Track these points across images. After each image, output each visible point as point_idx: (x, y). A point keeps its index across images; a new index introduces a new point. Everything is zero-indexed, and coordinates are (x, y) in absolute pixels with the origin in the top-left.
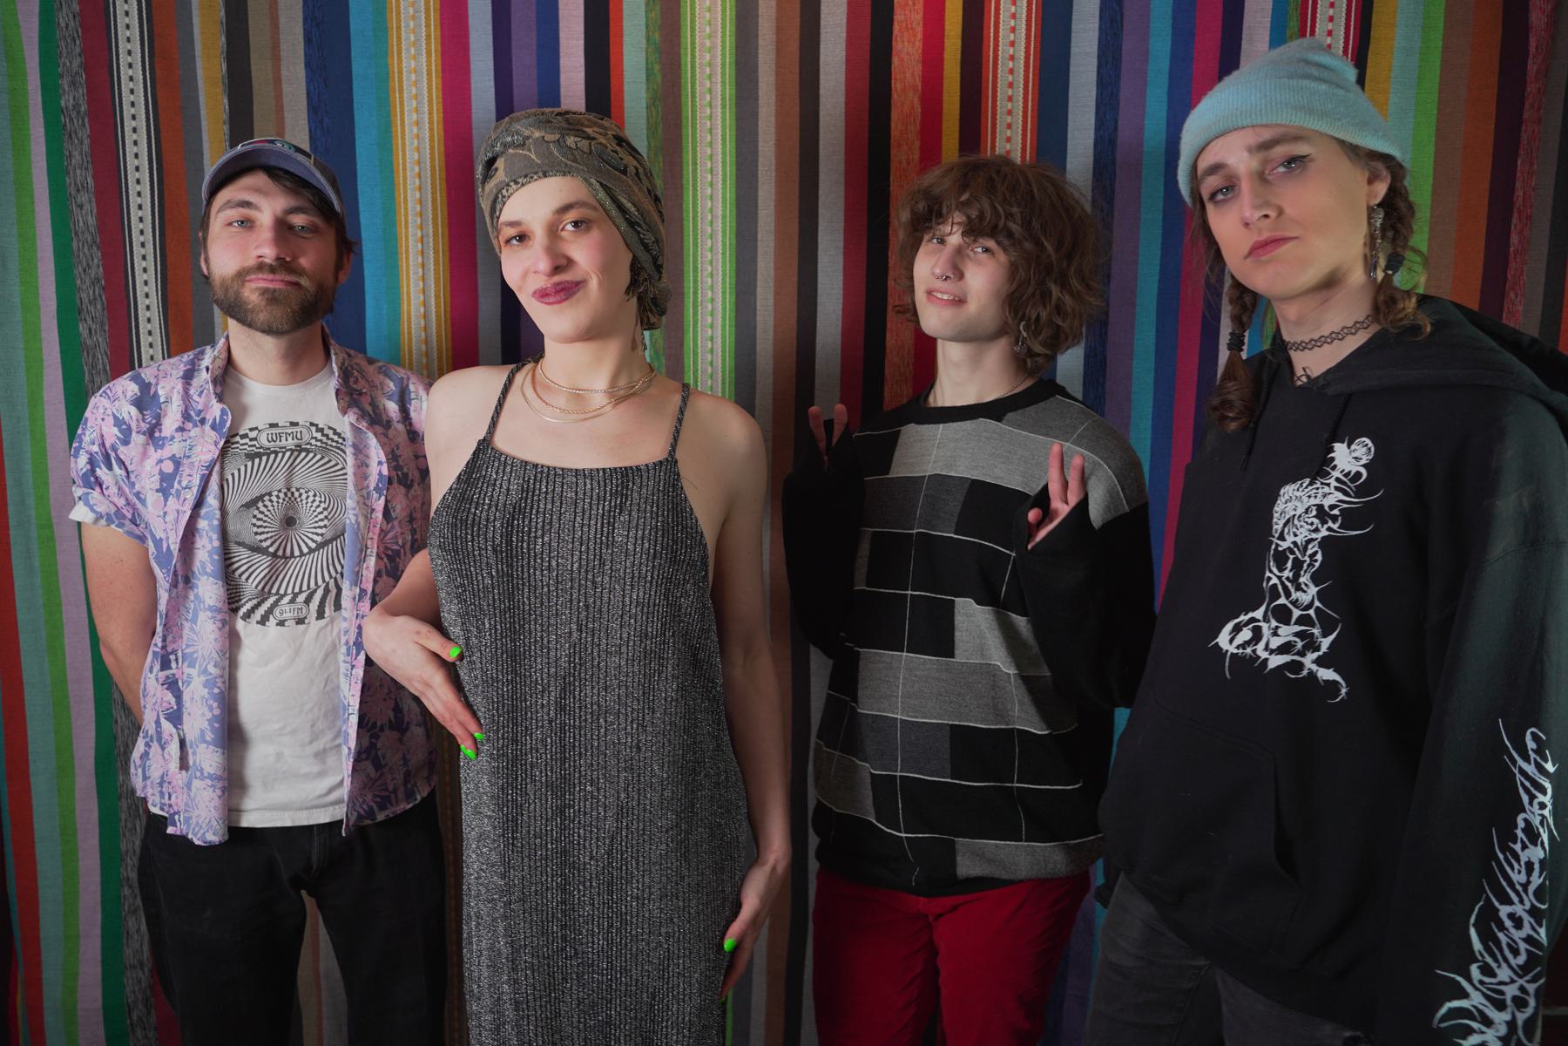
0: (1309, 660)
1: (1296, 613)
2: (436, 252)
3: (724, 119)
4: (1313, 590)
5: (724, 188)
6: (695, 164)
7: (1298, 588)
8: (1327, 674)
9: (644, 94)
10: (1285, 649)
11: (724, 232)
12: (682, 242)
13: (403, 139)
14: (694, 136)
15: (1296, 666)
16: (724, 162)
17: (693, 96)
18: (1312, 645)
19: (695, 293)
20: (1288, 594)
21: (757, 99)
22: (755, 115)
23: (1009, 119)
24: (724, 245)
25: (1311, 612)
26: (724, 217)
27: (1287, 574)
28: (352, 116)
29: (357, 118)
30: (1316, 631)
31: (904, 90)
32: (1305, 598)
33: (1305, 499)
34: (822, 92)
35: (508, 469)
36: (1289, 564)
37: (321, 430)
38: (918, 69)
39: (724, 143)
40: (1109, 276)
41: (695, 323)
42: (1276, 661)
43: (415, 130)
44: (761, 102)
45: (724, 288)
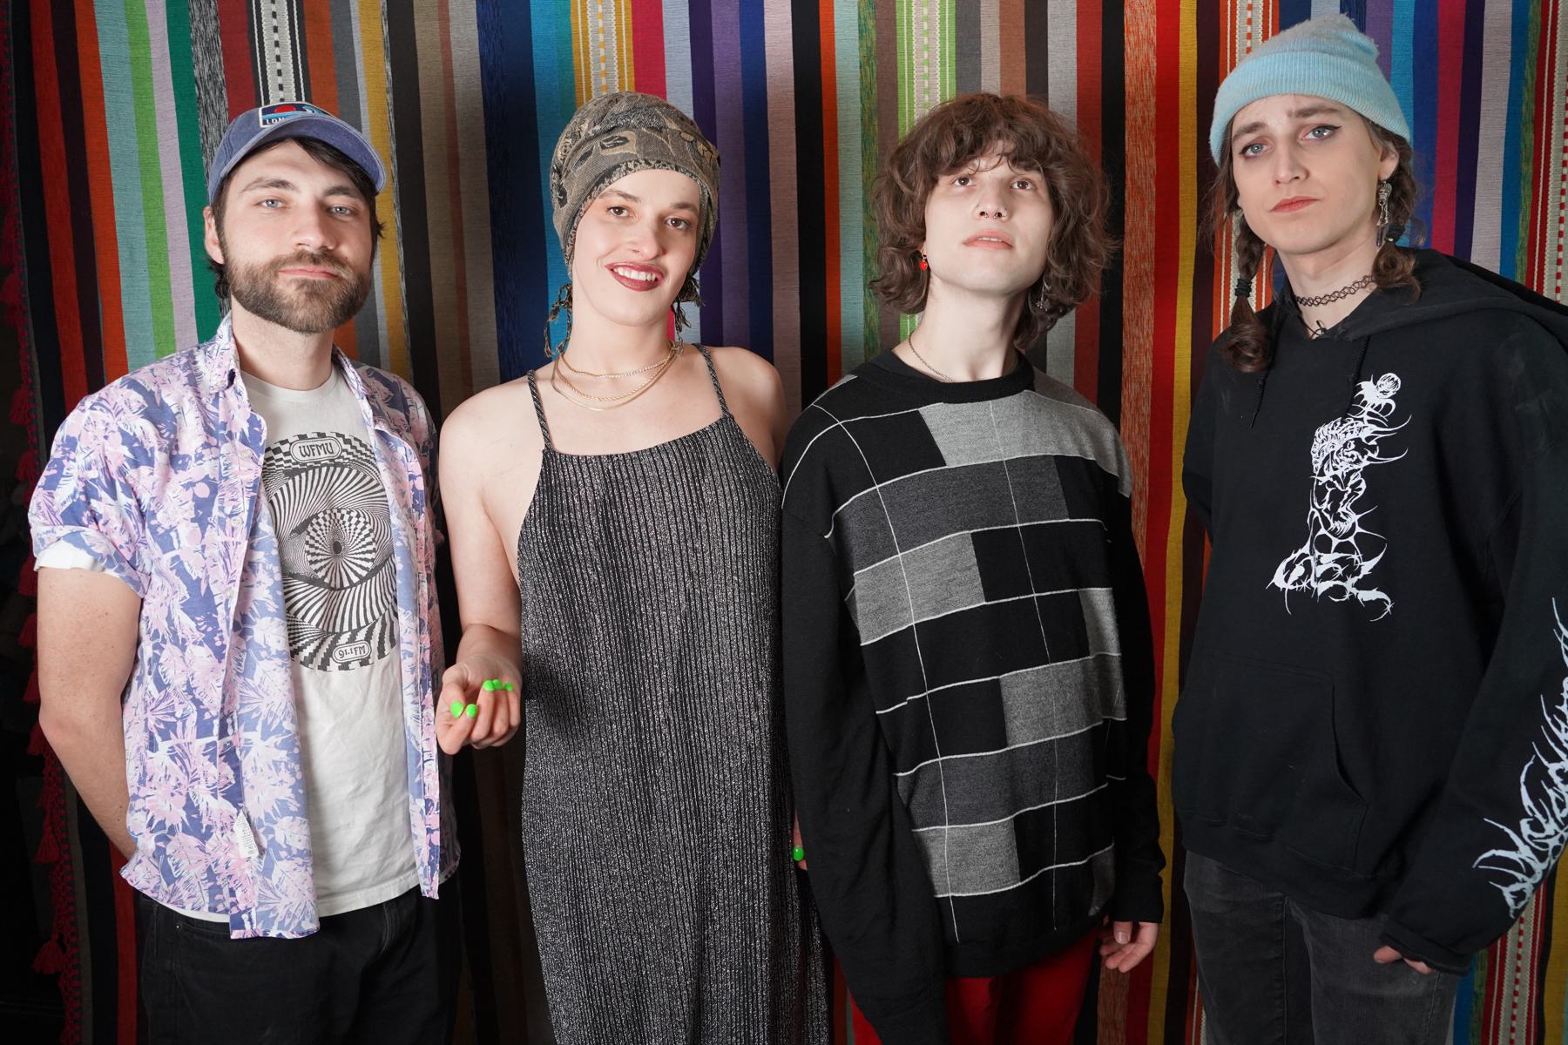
0: (1349, 584)
1: (1335, 542)
4: (1354, 518)
7: (1337, 518)
8: (1373, 595)
10: (1328, 575)
15: (1339, 591)
18: (1351, 570)
20: (1327, 525)
25: (1351, 539)
27: (1326, 505)
30: (1355, 557)
32: (1344, 527)
33: (1342, 436)
35: (585, 468)
36: (1327, 497)
37: (347, 442)
42: (1323, 587)
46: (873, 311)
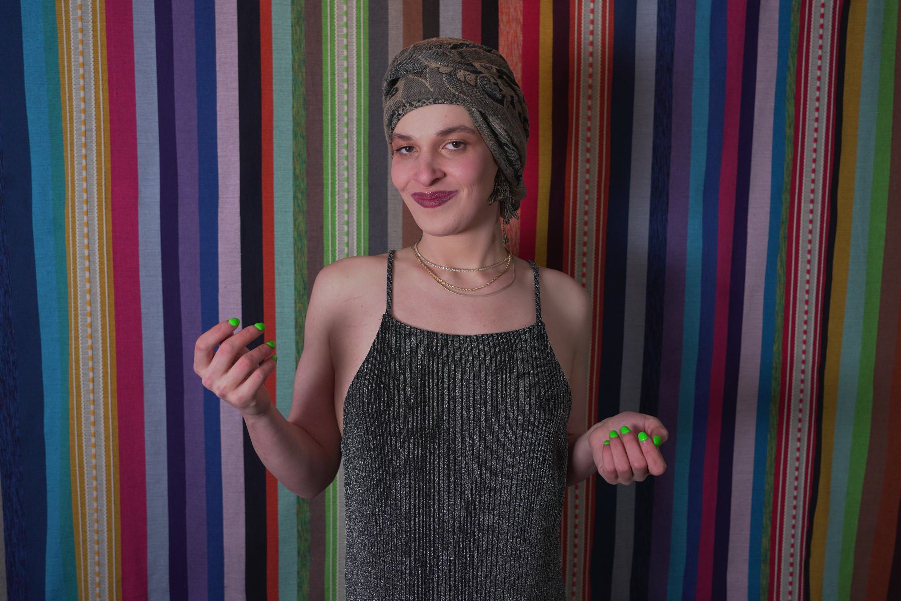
2: (98, 145)
3: (359, 38)
5: (359, 96)
6: (333, 74)
9: (290, 15)
11: (359, 133)
12: (322, 140)
13: (68, 44)
14: (332, 50)
16: (359, 74)
17: (332, 17)
19: (333, 184)
21: (387, 23)
22: (385, 36)
23: (590, 49)
24: (359, 143)
26: (359, 120)
28: (19, 21)
29: (24, 24)
31: (508, 22)
34: (442, 20)
38: (520, 5)
39: (359, 58)
40: (668, 174)
41: (334, 208)
43: (80, 36)
44: (390, 25)
45: (359, 180)
46: (300, 218)
